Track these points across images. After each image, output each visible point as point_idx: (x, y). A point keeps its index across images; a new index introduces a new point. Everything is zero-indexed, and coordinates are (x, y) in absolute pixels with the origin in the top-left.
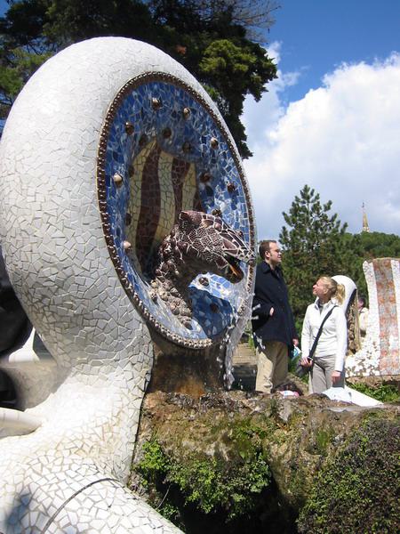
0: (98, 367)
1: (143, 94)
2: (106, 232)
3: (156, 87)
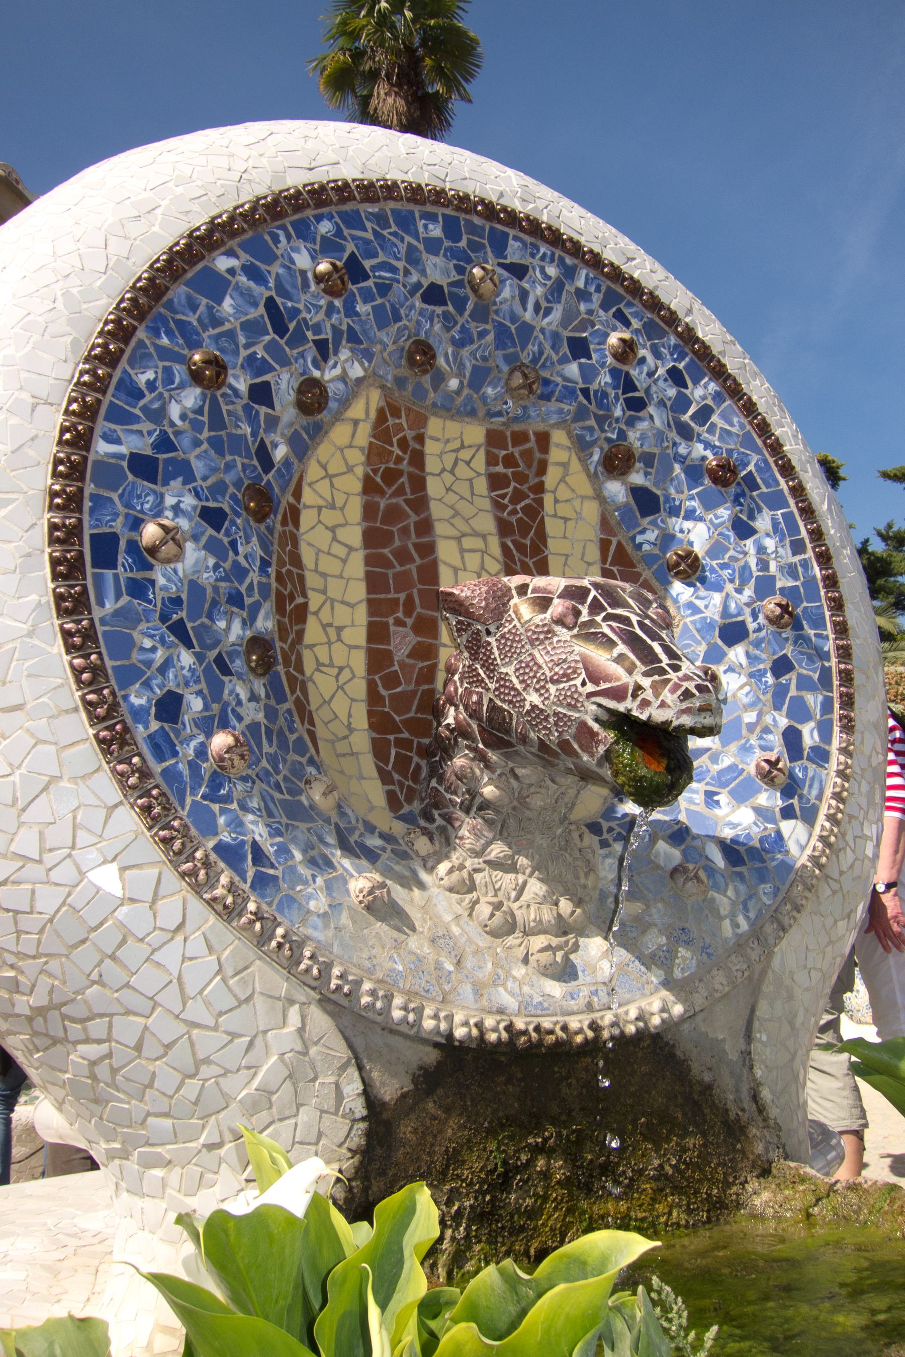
0: (158, 1173)
1: (270, 258)
3: (325, 228)
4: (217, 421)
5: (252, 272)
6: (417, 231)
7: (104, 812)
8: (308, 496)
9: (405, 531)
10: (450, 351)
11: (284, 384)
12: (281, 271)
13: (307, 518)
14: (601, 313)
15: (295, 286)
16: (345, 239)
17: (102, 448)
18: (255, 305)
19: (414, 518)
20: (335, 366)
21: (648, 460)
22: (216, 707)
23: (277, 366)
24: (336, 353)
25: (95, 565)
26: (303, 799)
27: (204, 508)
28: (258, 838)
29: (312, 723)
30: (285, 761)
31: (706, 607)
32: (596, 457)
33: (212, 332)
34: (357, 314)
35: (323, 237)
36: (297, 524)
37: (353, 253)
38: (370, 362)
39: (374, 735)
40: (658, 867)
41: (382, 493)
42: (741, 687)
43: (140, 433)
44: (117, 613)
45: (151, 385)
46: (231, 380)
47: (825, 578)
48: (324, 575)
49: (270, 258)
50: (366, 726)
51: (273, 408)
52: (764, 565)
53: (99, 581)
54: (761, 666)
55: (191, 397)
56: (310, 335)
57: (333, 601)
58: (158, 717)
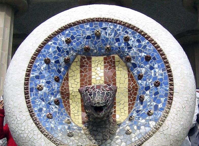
1: (57, 40)
2: (30, 112)
3: (67, 32)
4: (49, 68)
5: (55, 43)
6: (84, 27)
7: (31, 124)
8: (69, 75)
9: (87, 78)
10: (93, 46)
11: (62, 59)
12: (59, 42)
13: (70, 79)
14: (122, 32)
15: (62, 43)
16: (70, 33)
17: (31, 75)
18: (55, 48)
19: (88, 76)
20: (70, 54)
21: (134, 58)
22: (48, 109)
23: (59, 57)
24: (70, 52)
25: (30, 92)
26: (64, 122)
27: (47, 81)
28: (52, 127)
29: (70, 111)
30: (61, 117)
31: (143, 84)
32: (124, 59)
33: (48, 54)
34: (73, 45)
35: (67, 34)
36: (68, 80)
37: (72, 35)
38: (76, 52)
39: (82, 112)
40: (125, 130)
41: (83, 72)
42: (148, 98)
43: (37, 72)
44: (33, 98)
45: (38, 65)
46: (51, 61)
47: (169, 75)
48: (73, 88)
49: (57, 40)
50: (81, 111)
51: (60, 63)
52: (155, 74)
53: (31, 94)
54: (152, 94)
55: (45, 65)
56: (65, 51)
57: (74, 91)
58: (38, 111)
